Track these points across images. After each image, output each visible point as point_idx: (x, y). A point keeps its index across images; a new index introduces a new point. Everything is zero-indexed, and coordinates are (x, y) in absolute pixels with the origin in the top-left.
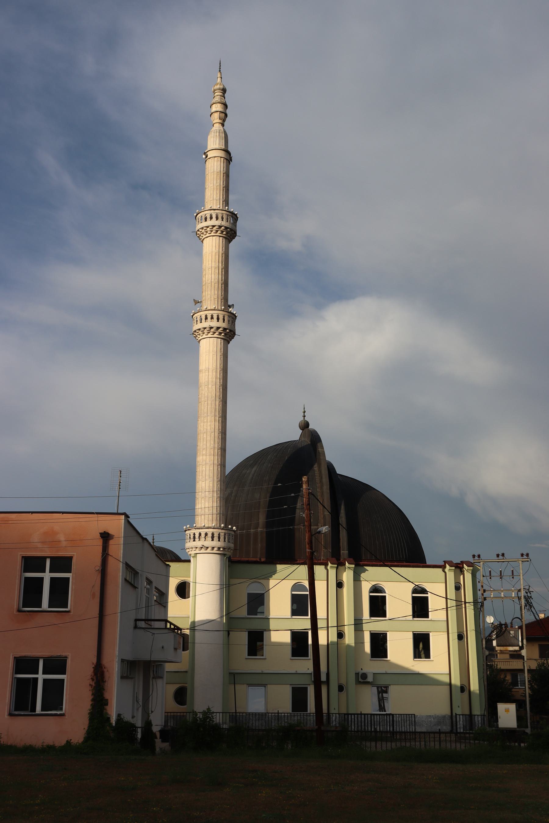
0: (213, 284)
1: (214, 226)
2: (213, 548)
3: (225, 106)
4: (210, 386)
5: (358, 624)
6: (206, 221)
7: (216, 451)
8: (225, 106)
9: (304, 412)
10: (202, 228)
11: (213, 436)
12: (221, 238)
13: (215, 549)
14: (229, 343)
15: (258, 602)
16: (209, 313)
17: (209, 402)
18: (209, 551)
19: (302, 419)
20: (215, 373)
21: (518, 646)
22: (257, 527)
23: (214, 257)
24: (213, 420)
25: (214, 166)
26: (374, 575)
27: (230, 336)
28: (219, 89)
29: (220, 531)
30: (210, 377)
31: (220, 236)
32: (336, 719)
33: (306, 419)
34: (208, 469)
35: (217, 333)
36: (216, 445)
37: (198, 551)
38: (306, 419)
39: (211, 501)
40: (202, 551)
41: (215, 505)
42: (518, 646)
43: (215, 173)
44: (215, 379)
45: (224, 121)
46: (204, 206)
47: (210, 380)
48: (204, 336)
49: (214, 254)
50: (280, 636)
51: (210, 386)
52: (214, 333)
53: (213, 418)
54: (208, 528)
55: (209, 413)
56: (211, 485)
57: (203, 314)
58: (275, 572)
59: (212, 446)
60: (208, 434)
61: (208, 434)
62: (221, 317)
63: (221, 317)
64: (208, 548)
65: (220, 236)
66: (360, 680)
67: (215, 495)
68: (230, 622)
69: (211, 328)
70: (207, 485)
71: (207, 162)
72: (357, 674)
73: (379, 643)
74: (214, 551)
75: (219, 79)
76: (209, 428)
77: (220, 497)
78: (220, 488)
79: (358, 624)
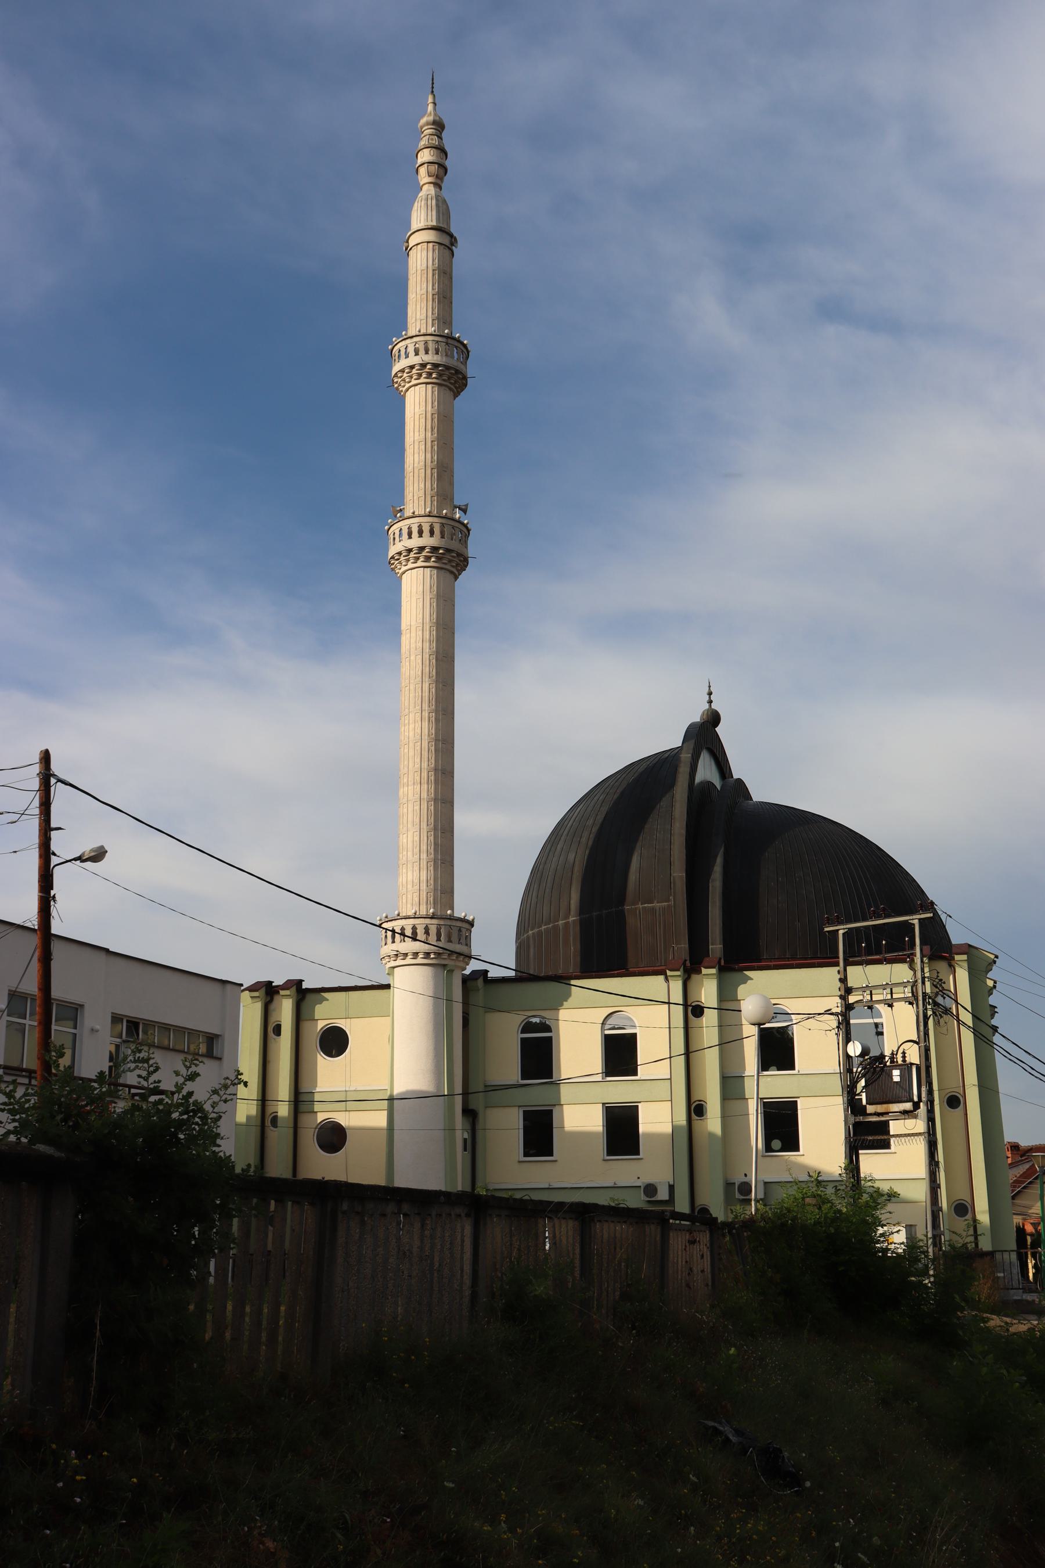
0: (416, 471)
1: (412, 367)
2: (416, 955)
3: (441, 150)
4: (413, 658)
5: (732, 1086)
6: (407, 356)
7: (425, 774)
8: (441, 150)
9: (710, 694)
10: (402, 371)
11: (419, 748)
12: (430, 387)
13: (421, 956)
14: (456, 578)
15: (539, 1056)
16: (414, 523)
17: (412, 688)
18: (408, 961)
19: (707, 706)
20: (420, 633)
21: (911, 1100)
22: (567, 917)
23: (417, 423)
24: (419, 719)
25: (420, 261)
26: (762, 991)
27: (457, 565)
28: (428, 124)
29: (428, 921)
30: (413, 640)
31: (427, 383)
32: (463, 1230)
33: (713, 706)
34: (410, 809)
35: (422, 559)
36: (425, 765)
37: (393, 964)
38: (713, 706)
39: (417, 868)
40: (399, 962)
41: (424, 877)
42: (911, 1100)
43: (419, 272)
44: (420, 644)
45: (442, 179)
46: (406, 330)
47: (413, 646)
48: (410, 565)
49: (417, 417)
50: (581, 1117)
51: (413, 658)
52: (418, 559)
53: (419, 715)
54: (406, 918)
55: (412, 706)
56: (417, 838)
57: (404, 524)
58: (567, 996)
59: (418, 766)
60: (411, 745)
61: (411, 745)
62: (437, 530)
63: (426, 529)
64: (406, 955)
65: (427, 383)
66: (738, 1196)
67: (424, 856)
68: (468, 1097)
69: (410, 551)
70: (410, 839)
71: (411, 253)
72: (729, 1185)
73: (782, 1124)
74: (419, 961)
75: (430, 107)
76: (411, 734)
77: (435, 861)
78: (436, 844)
79: (732, 1086)
